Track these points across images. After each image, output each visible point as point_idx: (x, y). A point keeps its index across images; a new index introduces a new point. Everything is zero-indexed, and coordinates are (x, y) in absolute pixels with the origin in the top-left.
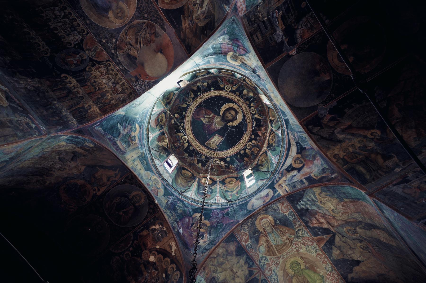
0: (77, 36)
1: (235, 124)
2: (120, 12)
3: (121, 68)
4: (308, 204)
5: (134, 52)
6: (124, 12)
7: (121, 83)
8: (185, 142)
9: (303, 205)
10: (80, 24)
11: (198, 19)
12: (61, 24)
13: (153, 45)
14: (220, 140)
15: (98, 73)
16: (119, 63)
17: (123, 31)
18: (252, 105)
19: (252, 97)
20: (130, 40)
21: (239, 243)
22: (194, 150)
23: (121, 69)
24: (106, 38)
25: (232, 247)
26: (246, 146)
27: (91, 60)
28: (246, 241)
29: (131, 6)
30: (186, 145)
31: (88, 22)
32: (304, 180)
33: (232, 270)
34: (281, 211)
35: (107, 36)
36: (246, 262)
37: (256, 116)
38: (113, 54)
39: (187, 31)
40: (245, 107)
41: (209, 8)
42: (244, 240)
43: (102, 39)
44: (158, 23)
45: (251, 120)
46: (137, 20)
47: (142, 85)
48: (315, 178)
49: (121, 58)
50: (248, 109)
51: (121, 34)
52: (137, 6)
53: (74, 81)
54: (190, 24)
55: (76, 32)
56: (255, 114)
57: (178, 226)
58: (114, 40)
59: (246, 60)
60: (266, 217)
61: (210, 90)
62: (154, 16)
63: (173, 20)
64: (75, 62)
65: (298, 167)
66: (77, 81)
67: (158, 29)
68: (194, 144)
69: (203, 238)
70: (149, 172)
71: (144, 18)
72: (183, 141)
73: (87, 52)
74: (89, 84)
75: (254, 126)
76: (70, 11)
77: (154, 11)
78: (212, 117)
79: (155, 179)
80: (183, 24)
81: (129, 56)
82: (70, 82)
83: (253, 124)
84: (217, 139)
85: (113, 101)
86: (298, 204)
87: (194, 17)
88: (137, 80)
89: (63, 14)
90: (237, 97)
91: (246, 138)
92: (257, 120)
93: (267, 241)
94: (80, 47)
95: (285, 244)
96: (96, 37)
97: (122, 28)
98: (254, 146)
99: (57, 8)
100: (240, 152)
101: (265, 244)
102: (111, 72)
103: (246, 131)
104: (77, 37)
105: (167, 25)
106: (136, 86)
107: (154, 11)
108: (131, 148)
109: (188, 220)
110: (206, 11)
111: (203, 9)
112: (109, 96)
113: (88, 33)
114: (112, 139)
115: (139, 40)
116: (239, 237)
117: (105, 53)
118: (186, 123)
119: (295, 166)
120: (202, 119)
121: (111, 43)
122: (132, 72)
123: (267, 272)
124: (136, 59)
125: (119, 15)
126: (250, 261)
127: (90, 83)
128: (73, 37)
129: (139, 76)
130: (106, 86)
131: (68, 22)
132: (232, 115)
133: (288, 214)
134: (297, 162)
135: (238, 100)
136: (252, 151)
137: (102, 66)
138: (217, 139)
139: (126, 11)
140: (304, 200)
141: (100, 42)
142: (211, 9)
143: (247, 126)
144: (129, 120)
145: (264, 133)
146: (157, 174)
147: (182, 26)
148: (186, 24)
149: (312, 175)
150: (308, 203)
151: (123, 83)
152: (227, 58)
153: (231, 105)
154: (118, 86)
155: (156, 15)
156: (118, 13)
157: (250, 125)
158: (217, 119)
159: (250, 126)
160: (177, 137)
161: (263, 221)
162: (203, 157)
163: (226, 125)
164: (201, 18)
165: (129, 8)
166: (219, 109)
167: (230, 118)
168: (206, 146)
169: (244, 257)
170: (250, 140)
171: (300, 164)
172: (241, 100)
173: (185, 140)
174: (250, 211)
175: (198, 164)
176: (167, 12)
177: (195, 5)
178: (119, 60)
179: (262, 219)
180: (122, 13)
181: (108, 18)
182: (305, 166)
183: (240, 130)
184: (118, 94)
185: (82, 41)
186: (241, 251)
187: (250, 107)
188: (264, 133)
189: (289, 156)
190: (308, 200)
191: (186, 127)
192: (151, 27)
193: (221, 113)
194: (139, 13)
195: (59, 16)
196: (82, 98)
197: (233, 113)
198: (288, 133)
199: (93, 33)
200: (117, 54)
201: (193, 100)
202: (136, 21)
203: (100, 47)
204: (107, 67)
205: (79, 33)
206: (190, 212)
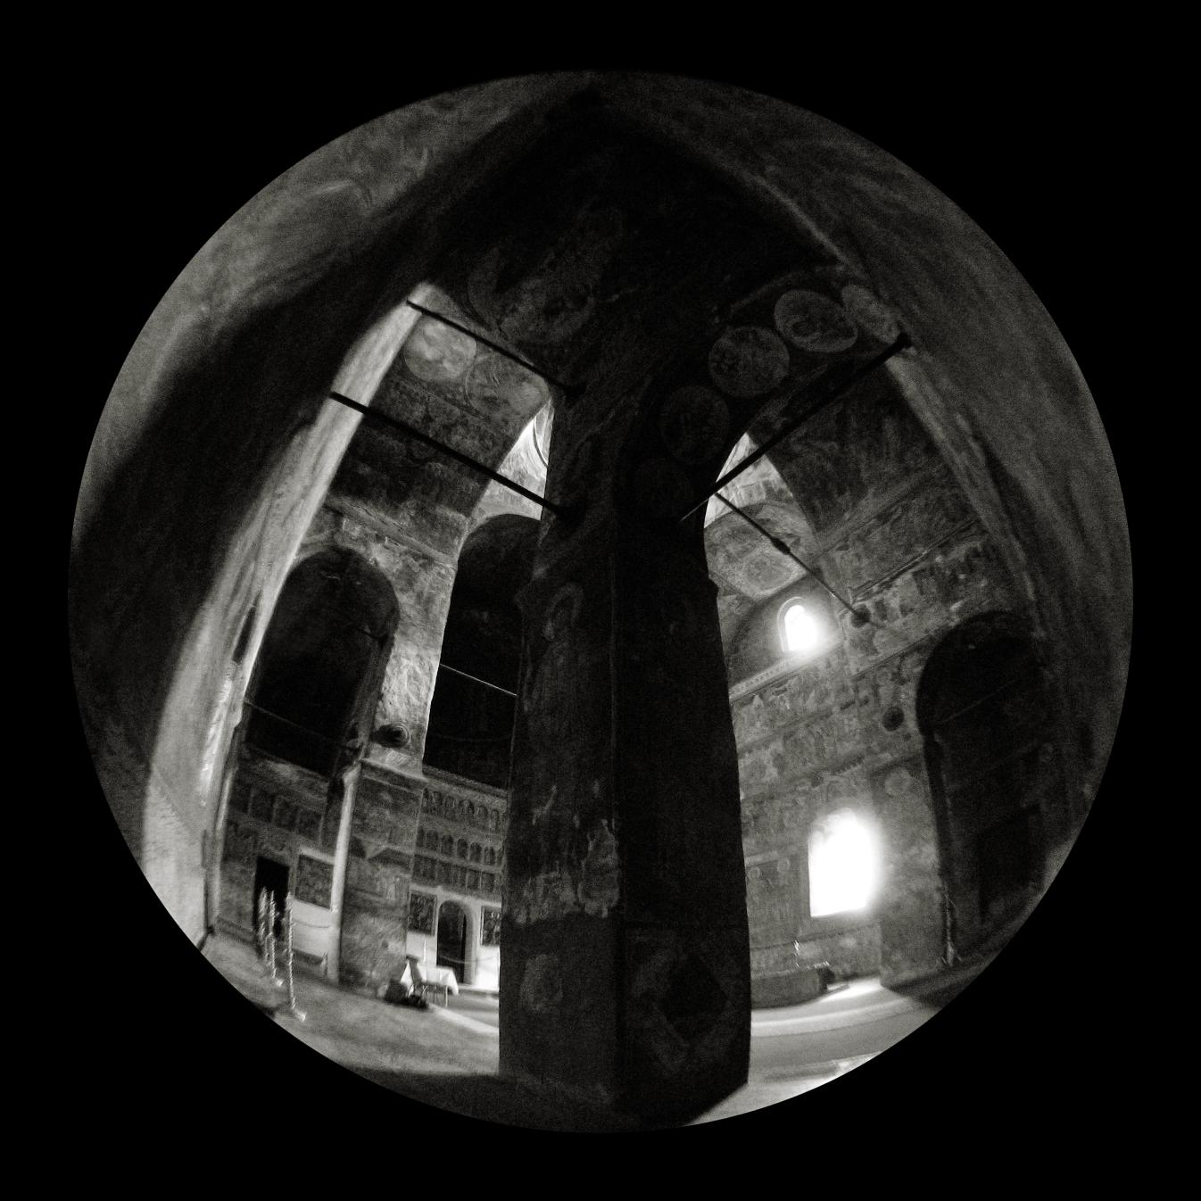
5: (489, 393)
13: (513, 378)
16: (477, 413)
31: (425, 385)
38: (466, 406)
53: (440, 465)
73: (437, 419)
81: (486, 400)
88: (506, 422)
94: (428, 419)
95: (747, 549)
122: (498, 416)
129: (506, 417)
141: (446, 399)
185: (427, 410)
202: (480, 359)
203: (449, 407)
204: (465, 424)
205: (421, 404)
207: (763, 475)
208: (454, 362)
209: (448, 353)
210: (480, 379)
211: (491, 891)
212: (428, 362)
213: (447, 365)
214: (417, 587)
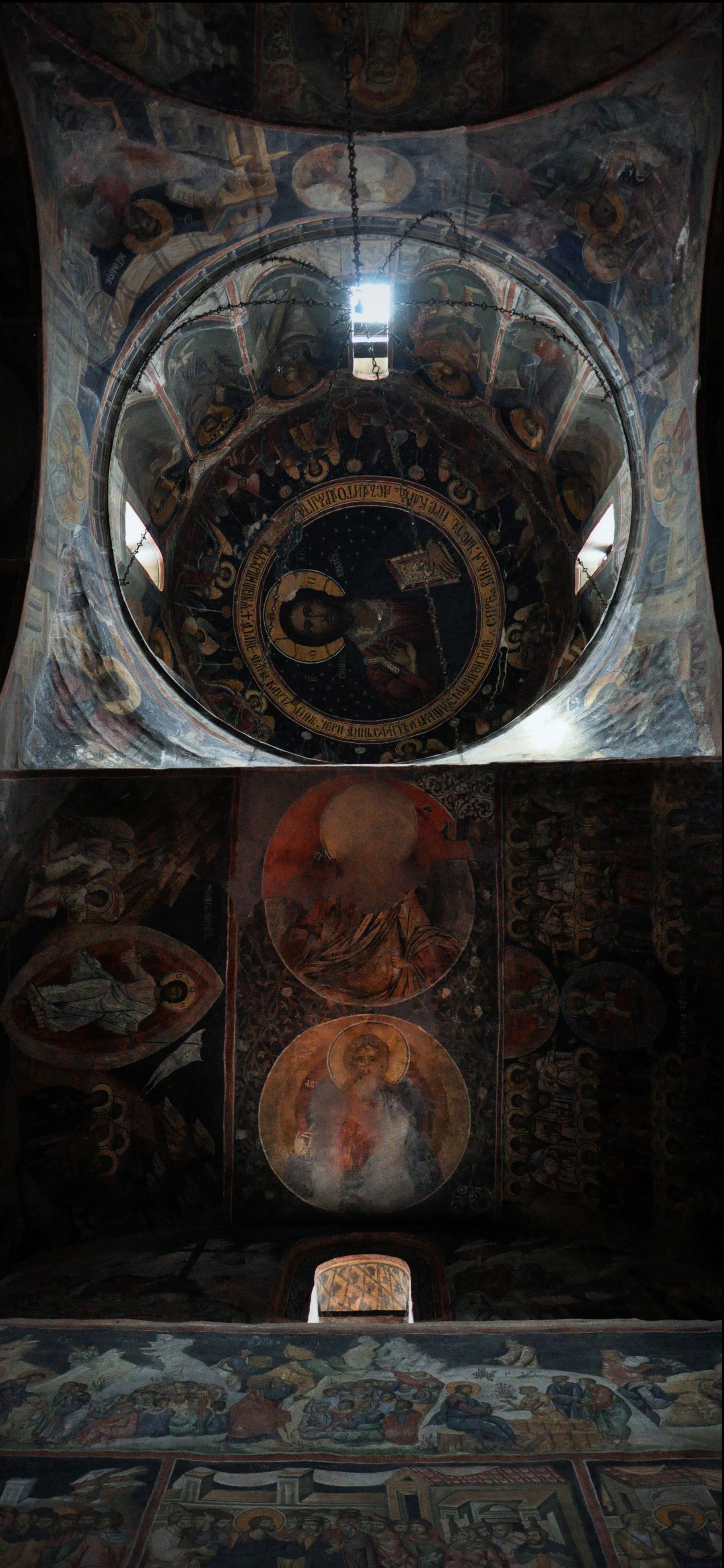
0: (546, 1073)
1: (319, 581)
2: (361, 1059)
3: (487, 894)
4: (196, 42)
5: (412, 917)
6: (349, 1049)
7: (525, 845)
8: (518, 627)
9: (213, 51)
10: (509, 1102)
11: (123, 851)
12: (566, 1132)
14: (403, 562)
15: (570, 922)
16: (483, 912)
17: (396, 1000)
18: (216, 594)
19: (198, 615)
20: (396, 959)
22: (508, 582)
23: (491, 889)
24: (463, 1015)
26: (327, 478)
27: (560, 977)
29: (313, 1049)
30: (521, 615)
31: (483, 1094)
32: (158, 135)
34: (303, 81)
35: (456, 1020)
37: (227, 549)
38: (479, 954)
39: (184, 850)
40: (245, 606)
41: (59, 848)
42: (488, 63)
43: (480, 1022)
44: (266, 942)
45: (256, 548)
46: (325, 1001)
47: (460, 796)
48: (117, 116)
49: (466, 923)
50: (239, 593)
51: (410, 996)
52: (293, 1036)
53: (659, 932)
54: (160, 858)
55: (541, 1086)
56: (225, 558)
57: (681, 261)
58: (446, 992)
59: (79, 651)
61: (316, 737)
62: (264, 973)
63: (208, 917)
64: (612, 995)
65: (159, 206)
66: (649, 928)
67: (277, 928)
68: (496, 604)
69: (627, 169)
70: (663, 521)
71: (299, 989)
72: (522, 632)
74: (622, 900)
75: (257, 525)
76: (509, 1149)
77: (252, 987)
78: (375, 655)
79: (660, 484)
80: (182, 880)
82: (673, 935)
83: (257, 533)
84: (413, 571)
85: (589, 799)
86: (228, 66)
87: (129, 867)
88: (465, 823)
89: (537, 1154)
90: (249, 655)
91: (314, 506)
92: (235, 535)
94: (563, 1037)
96: (492, 1037)
97: (391, 1011)
98: (300, 457)
99: (540, 1178)
100: (361, 473)
102: (527, 901)
103: (298, 527)
104: (550, 1069)
105: (238, 914)
106: (483, 805)
107: (252, 987)
108: (661, 637)
109: (642, 271)
110: (75, 845)
111: (81, 859)
112: (590, 826)
113: (508, 1062)
114: (694, 694)
115: (368, 940)
117: (502, 972)
118: (473, 687)
119: (167, 217)
120: (413, 668)
121: (461, 992)
124: (418, 891)
125: (372, 1053)
127: (616, 901)
128: (563, 1075)
130: (576, 864)
131: (539, 1126)
132: (307, 612)
133: (285, 55)
134: (153, 225)
135: (251, 645)
136: (318, 443)
137: (541, 938)
138: (413, 571)
139: (340, 1047)
140: (197, 62)
141: (491, 1015)
142: (54, 838)
143: (282, 542)
144: (599, 729)
145: (238, 469)
146: (646, 504)
147: (192, 878)
148: (175, 872)
149: (122, 137)
150: (189, 44)
151: (516, 839)
152: (137, 704)
153: (287, 648)
154: (541, 843)
155: (257, 970)
156: (373, 1059)
157: (270, 537)
158: (365, 638)
159: (269, 532)
160: (531, 656)
161: (383, 89)
162: (495, 535)
163: (348, 598)
164: (109, 844)
165: (322, 1049)
166: (335, 660)
167: (318, 609)
168: (463, 570)
170: (300, 488)
171: (145, 214)
172: (242, 636)
173: (514, 632)
174: (409, 153)
175: (524, 523)
176: (212, 950)
177: (103, 896)
178: (476, 923)
179: (380, 94)
180: (358, 1050)
181: (412, 1066)
182: (132, 190)
183: (314, 546)
184: (559, 816)
185: (542, 1052)
187: (228, 593)
188: (238, 469)
189: (168, 270)
190: (185, 51)
191: (480, 676)
192: (295, 951)
193: (336, 647)
194: (303, 1013)
195: (548, 1156)
197: (298, 618)
198: (120, 345)
199: (493, 1052)
200: (469, 946)
201: (395, 744)
202: (333, 999)
203: (504, 999)
205: (534, 1078)
206: (620, 296)
207: (144, 157)
208: (384, 1053)
209: (368, 1086)
210: (390, 965)
212: (421, 1122)
213: (397, 1072)
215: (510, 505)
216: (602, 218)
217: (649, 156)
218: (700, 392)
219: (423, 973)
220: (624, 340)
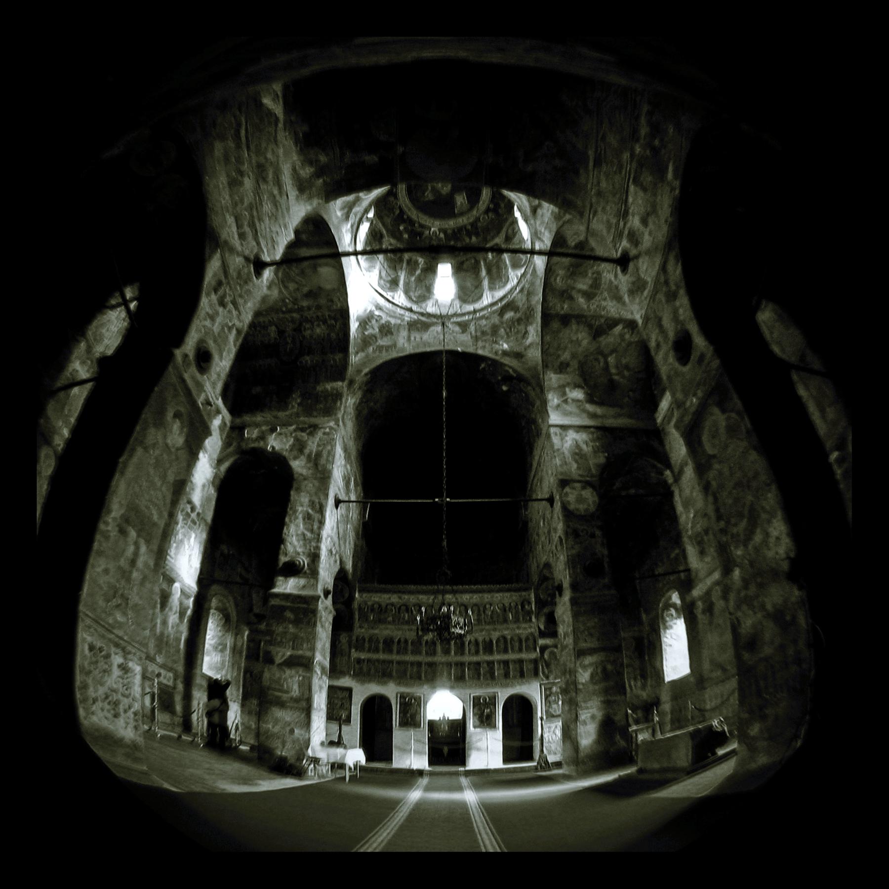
5: (306, 290)
16: (309, 308)
21: (557, 315)
25: (555, 325)
27: (295, 330)
28: (563, 308)
33: (572, 341)
36: (578, 323)
53: (308, 358)
60: (558, 275)
66: (308, 355)
68: (447, 226)
84: (461, 200)
88: (332, 301)
93: (579, 291)
94: (281, 332)
101: (580, 295)
116: (552, 312)
122: (323, 301)
123: (603, 313)
126: (580, 318)
138: (461, 200)
169: (573, 321)
185: (276, 326)
186: (565, 320)
196: (323, 361)
202: (280, 275)
203: (287, 316)
210: (292, 286)
211: (479, 678)
214: (307, 451)
215: (477, 235)
216: (519, 321)
217: (529, 341)
218: (457, 352)
219: (290, 293)
220: (487, 318)
